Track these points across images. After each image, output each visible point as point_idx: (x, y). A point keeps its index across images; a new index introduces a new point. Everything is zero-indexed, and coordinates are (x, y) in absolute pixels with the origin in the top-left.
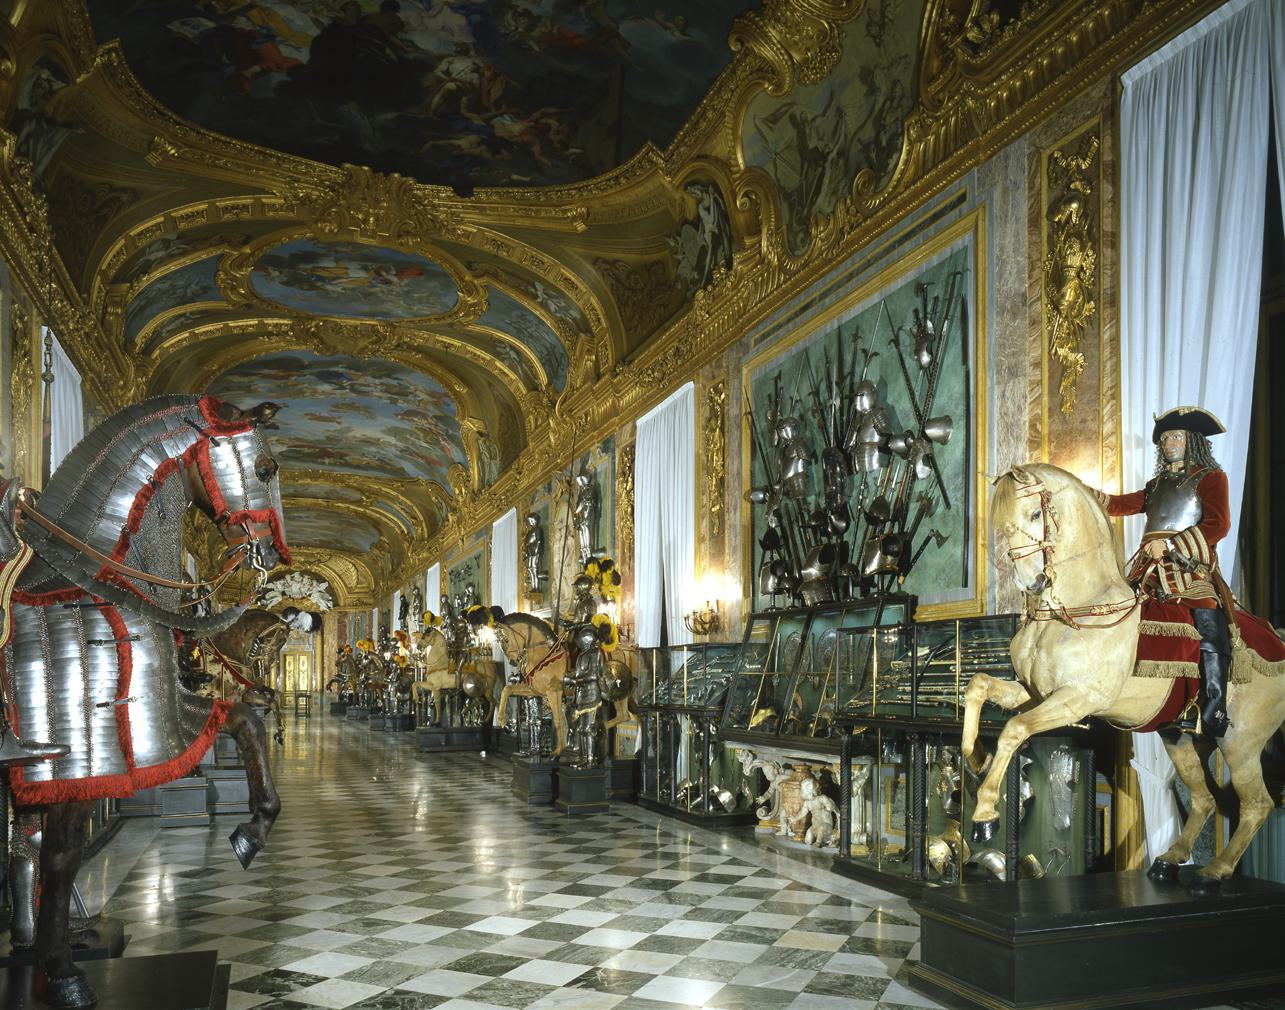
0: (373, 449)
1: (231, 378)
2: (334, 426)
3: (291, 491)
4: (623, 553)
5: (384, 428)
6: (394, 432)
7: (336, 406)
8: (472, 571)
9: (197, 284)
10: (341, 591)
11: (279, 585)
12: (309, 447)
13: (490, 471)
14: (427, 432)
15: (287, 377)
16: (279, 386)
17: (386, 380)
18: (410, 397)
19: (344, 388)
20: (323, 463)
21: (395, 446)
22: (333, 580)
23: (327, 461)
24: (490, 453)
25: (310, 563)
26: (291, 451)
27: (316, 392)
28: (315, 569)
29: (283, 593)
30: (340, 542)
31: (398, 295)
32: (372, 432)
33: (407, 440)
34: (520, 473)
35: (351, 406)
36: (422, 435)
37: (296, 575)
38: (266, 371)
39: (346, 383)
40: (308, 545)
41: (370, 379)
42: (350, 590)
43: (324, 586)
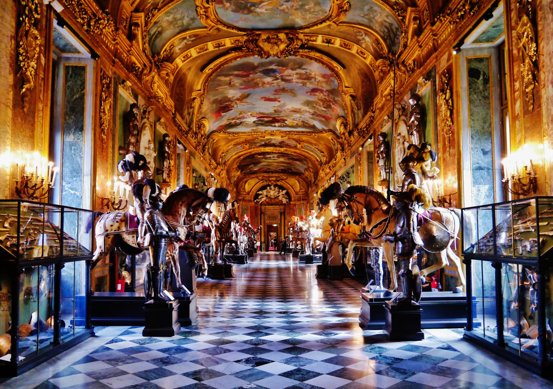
0: (298, 115)
1: (219, 78)
2: (276, 104)
3: (263, 143)
4: (444, 144)
5: (302, 102)
6: (308, 103)
7: (276, 91)
8: (350, 175)
9: (187, 17)
10: (293, 194)
11: (265, 192)
12: (267, 117)
13: (358, 117)
15: (247, 76)
16: (245, 81)
17: (298, 71)
18: (313, 80)
19: (277, 79)
20: (275, 126)
22: (289, 189)
23: (277, 124)
24: (357, 106)
25: (278, 181)
27: (264, 83)
28: (279, 183)
29: (267, 196)
30: (291, 170)
31: (296, 9)
33: (314, 107)
34: (374, 112)
35: (284, 90)
36: (321, 103)
37: (272, 187)
38: (236, 72)
39: (278, 75)
40: (276, 172)
42: (297, 193)
43: (284, 192)
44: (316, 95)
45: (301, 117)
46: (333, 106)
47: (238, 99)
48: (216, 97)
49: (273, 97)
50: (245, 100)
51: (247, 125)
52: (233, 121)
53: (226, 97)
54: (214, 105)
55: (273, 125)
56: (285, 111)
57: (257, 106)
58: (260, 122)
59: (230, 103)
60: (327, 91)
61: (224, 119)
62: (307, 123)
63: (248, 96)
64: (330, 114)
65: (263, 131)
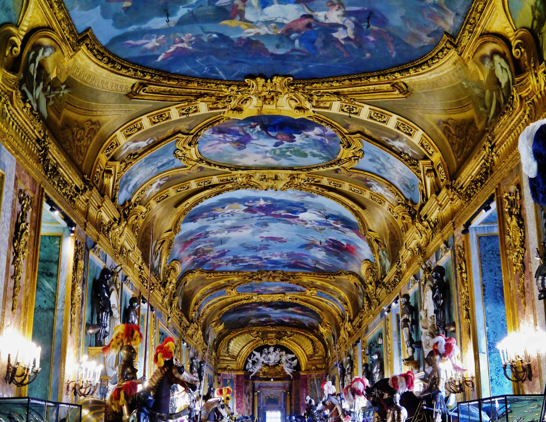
0: (228, 223)
2: (265, 234)
3: (299, 139)
6: (222, 242)
12: (280, 215)
14: (205, 252)
20: (265, 199)
21: (215, 233)
23: (262, 203)
26: (294, 212)
27: (280, 256)
32: (234, 235)
36: (206, 249)
41: (254, 263)
44: (217, 252)
45: (223, 221)
46: (193, 257)
47: (316, 246)
48: (338, 261)
49: (271, 242)
50: (308, 242)
51: (320, 209)
52: (339, 226)
53: (327, 254)
54: (346, 258)
55: (269, 203)
56: (252, 226)
57: (294, 233)
58: (295, 209)
59: (328, 247)
60: (209, 260)
61: (348, 238)
62: (207, 217)
63: (302, 247)
64: (187, 250)
65: (290, 191)
